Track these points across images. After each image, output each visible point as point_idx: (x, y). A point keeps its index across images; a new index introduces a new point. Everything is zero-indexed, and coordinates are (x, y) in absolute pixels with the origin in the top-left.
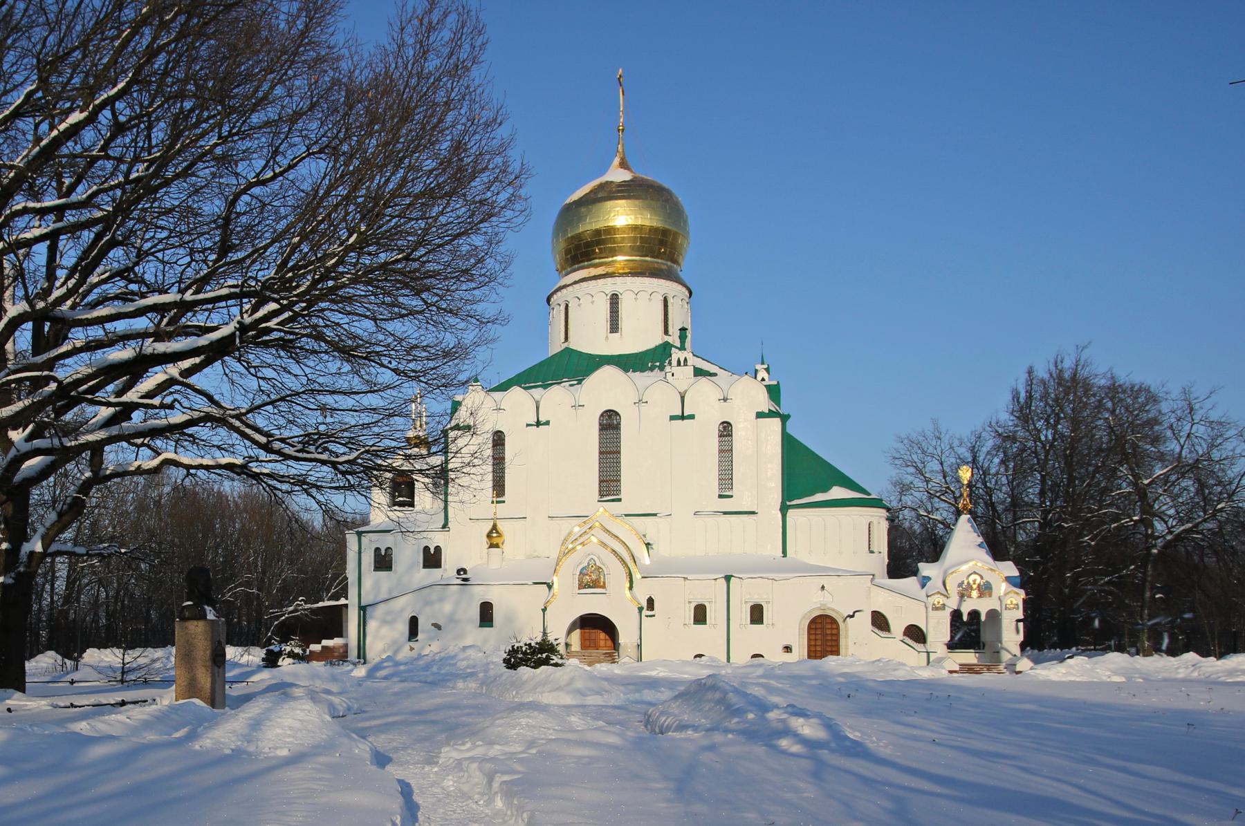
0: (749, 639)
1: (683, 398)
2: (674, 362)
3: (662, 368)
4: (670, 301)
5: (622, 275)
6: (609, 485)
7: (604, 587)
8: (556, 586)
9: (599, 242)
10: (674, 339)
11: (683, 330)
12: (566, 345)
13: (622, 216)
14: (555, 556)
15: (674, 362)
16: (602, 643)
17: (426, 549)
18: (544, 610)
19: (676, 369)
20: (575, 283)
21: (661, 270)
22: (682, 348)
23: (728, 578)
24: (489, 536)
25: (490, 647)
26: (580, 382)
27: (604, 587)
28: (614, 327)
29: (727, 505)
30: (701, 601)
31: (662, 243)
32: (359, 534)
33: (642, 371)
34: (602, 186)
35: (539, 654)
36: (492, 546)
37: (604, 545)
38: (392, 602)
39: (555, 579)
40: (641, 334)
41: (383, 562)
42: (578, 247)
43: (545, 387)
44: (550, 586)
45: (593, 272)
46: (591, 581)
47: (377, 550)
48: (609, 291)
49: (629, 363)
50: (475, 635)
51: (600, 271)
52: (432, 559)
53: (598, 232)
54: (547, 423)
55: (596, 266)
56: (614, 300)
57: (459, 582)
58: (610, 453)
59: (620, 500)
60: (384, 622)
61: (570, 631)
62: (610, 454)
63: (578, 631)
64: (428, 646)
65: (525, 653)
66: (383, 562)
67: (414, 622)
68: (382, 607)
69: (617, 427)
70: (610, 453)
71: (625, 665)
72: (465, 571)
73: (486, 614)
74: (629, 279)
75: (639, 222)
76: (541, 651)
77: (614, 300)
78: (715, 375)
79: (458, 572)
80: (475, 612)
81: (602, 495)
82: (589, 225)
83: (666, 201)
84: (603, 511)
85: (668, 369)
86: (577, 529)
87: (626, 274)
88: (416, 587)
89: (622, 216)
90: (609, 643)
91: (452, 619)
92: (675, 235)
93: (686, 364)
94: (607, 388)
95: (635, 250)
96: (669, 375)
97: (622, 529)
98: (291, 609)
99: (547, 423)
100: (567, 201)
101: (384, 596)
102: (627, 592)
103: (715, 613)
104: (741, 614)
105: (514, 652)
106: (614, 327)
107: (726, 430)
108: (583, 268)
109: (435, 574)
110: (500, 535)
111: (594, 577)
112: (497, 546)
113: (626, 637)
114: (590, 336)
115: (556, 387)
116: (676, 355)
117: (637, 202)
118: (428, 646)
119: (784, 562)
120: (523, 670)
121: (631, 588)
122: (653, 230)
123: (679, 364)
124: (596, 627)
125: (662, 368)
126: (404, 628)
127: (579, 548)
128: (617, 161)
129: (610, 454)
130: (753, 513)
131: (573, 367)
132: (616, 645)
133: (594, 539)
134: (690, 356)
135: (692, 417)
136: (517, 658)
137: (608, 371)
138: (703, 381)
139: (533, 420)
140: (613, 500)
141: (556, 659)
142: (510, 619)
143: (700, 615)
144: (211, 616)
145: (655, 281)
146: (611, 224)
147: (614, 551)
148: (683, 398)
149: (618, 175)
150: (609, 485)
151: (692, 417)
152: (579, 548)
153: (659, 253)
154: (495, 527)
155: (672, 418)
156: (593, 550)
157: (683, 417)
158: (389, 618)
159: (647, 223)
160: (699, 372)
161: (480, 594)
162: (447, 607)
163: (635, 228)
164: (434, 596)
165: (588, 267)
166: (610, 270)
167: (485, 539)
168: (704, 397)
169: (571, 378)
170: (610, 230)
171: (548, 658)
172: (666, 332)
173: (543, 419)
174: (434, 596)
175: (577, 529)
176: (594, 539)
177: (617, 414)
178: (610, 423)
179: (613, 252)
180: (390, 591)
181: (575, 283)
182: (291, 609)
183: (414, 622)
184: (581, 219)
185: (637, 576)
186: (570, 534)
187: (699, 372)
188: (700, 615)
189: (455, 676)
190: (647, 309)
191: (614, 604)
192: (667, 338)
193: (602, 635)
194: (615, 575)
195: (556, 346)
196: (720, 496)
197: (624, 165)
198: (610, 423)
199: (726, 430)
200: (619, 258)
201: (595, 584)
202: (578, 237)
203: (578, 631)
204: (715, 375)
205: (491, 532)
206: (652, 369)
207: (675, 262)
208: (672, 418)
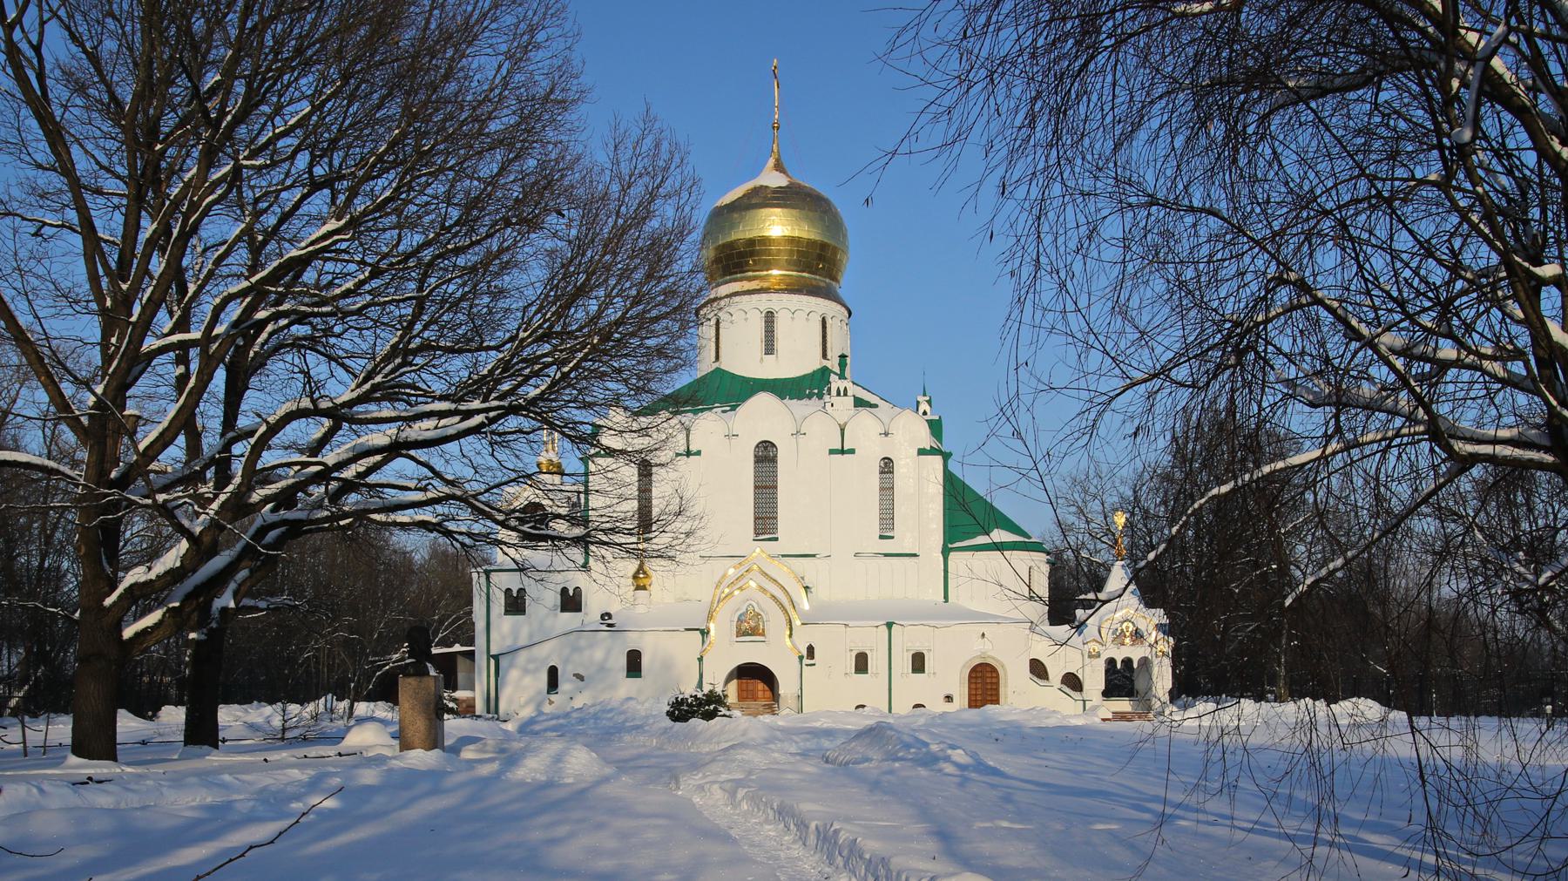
0: (911, 690)
1: (842, 431)
2: (834, 392)
3: (820, 396)
4: (829, 322)
5: (777, 291)
6: (765, 523)
8: (712, 633)
9: (752, 254)
10: (833, 364)
11: (843, 357)
13: (777, 225)
14: (707, 599)
15: (834, 392)
16: (760, 694)
17: (564, 591)
18: (700, 659)
19: (835, 400)
22: (842, 376)
23: (889, 625)
24: (635, 577)
25: (646, 699)
26: (733, 408)
28: (770, 348)
29: (888, 546)
30: (862, 649)
31: (821, 258)
32: (487, 573)
33: (800, 398)
34: (757, 191)
35: (707, 706)
36: (638, 588)
37: (763, 590)
38: (535, 649)
39: (712, 626)
40: (797, 355)
41: (515, 604)
42: (729, 257)
43: (695, 412)
44: (704, 633)
45: (747, 285)
46: (749, 628)
47: (508, 591)
48: (764, 307)
50: (627, 687)
52: (571, 601)
53: (751, 242)
54: (698, 453)
55: (750, 279)
56: (770, 318)
60: (526, 671)
61: (728, 681)
62: (766, 489)
65: (690, 705)
66: (515, 604)
67: (553, 673)
68: (522, 657)
69: (774, 460)
71: (785, 716)
72: (609, 615)
73: (634, 664)
74: (785, 297)
75: (796, 234)
77: (770, 318)
78: (876, 406)
79: (602, 617)
80: (623, 661)
81: (757, 534)
83: (825, 212)
84: (759, 551)
85: (827, 398)
86: (731, 571)
88: (560, 631)
89: (777, 225)
90: (769, 694)
91: (602, 669)
92: (835, 250)
94: (763, 417)
95: (791, 264)
97: (780, 570)
98: (395, 657)
99: (698, 453)
100: (718, 204)
101: (522, 642)
103: (876, 662)
104: (903, 662)
106: (770, 348)
107: (887, 466)
108: (736, 280)
110: (647, 575)
111: (752, 624)
112: (644, 588)
113: (786, 687)
115: (706, 414)
117: (794, 212)
119: (946, 611)
120: (696, 722)
122: (811, 243)
123: (838, 394)
124: (754, 676)
125: (820, 396)
126: (544, 677)
128: (771, 162)
129: (766, 489)
130: (915, 555)
131: (729, 391)
134: (849, 385)
135: (852, 451)
136: (681, 711)
137: (764, 400)
138: (864, 413)
139: (682, 449)
141: (723, 711)
142: (667, 666)
143: (861, 663)
144: (433, 673)
145: (812, 300)
148: (842, 431)
149: (773, 179)
150: (765, 523)
151: (852, 451)
153: (817, 268)
155: (832, 452)
157: (842, 452)
158: (531, 666)
159: (805, 235)
161: (633, 641)
162: (599, 654)
163: (792, 240)
164: (583, 643)
165: (741, 280)
166: (765, 285)
169: (723, 403)
170: (765, 241)
171: (716, 710)
172: (824, 356)
173: (693, 448)
174: (583, 643)
175: (731, 571)
176: (753, 584)
177: (773, 445)
178: (766, 455)
179: (768, 265)
180: (531, 636)
182: (395, 657)
184: (733, 226)
185: (797, 622)
186: (724, 576)
187: (859, 403)
188: (861, 663)
189: (620, 729)
190: (801, 331)
191: (775, 653)
192: (825, 363)
193: (761, 686)
194: (774, 621)
195: (705, 366)
196: (881, 537)
197: (779, 167)
198: (766, 455)
199: (887, 466)
200: (775, 272)
201: (754, 631)
204: (876, 406)
205: (638, 572)
206: (810, 397)
207: (835, 279)
208: (832, 452)
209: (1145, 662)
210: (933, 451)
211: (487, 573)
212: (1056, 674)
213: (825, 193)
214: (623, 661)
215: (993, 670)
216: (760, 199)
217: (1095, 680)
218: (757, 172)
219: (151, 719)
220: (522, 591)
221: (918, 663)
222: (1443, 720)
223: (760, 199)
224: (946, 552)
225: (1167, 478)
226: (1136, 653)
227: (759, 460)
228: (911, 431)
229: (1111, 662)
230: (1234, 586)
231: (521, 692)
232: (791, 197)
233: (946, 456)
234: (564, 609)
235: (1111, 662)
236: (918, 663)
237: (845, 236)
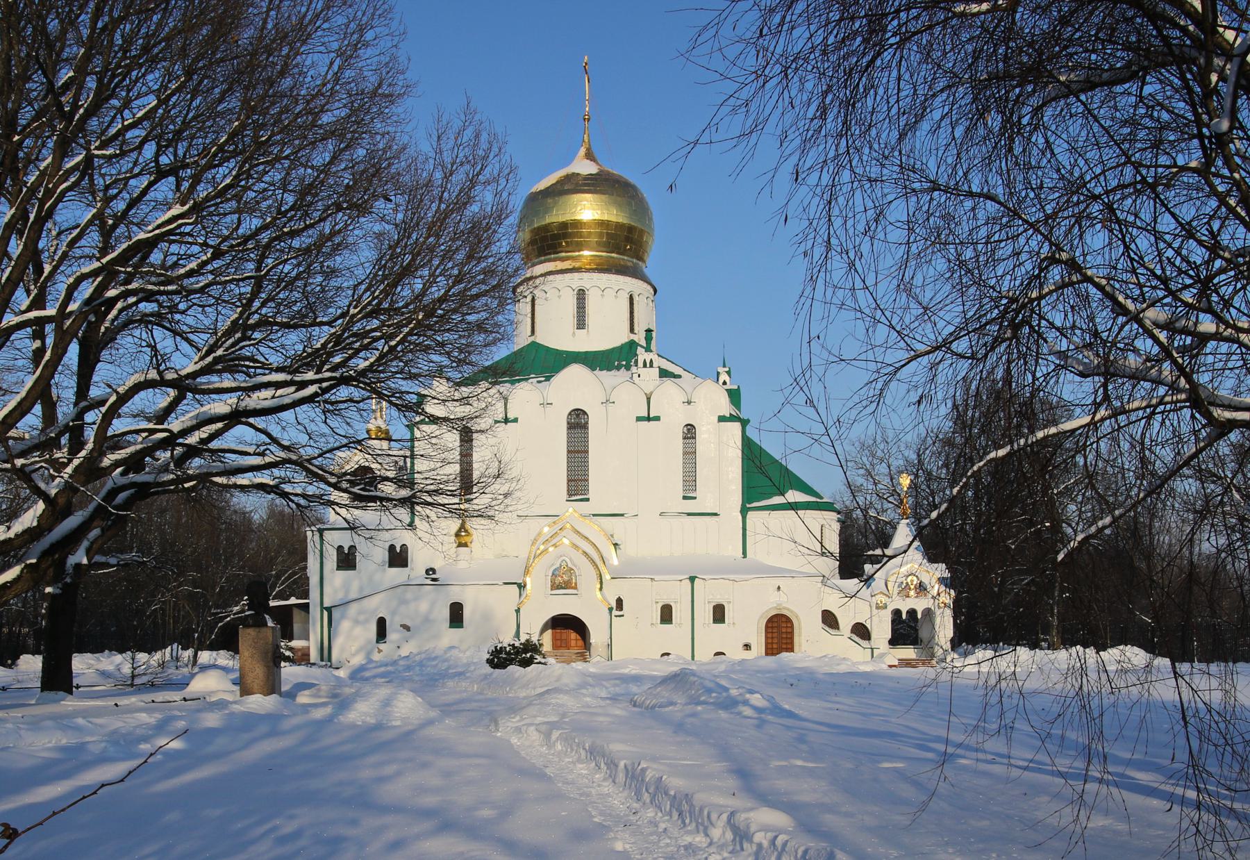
0: (712, 638)
1: (649, 399)
2: (640, 364)
3: (628, 368)
4: (636, 299)
5: (588, 270)
6: (577, 485)
7: (575, 588)
8: (528, 587)
9: (565, 236)
10: (640, 338)
11: (649, 331)
12: (532, 339)
13: (587, 210)
14: (524, 555)
15: (640, 364)
16: (573, 643)
17: (392, 548)
18: (518, 611)
19: (642, 371)
21: (627, 267)
22: (648, 349)
23: (692, 579)
24: (457, 535)
25: (468, 648)
26: (548, 379)
27: (575, 588)
28: (581, 324)
29: (691, 506)
30: (667, 602)
31: (628, 240)
32: (321, 531)
33: (609, 370)
34: (569, 178)
35: (524, 654)
36: (460, 545)
37: (575, 546)
38: (365, 601)
39: (528, 580)
40: (606, 332)
41: (347, 560)
42: (544, 239)
43: (513, 383)
44: (522, 587)
46: (563, 582)
47: (340, 548)
49: (597, 361)
50: (451, 636)
51: (567, 265)
52: (398, 558)
53: (564, 225)
54: (516, 420)
55: (563, 259)
56: (581, 295)
57: (429, 582)
58: (578, 452)
59: (588, 500)
60: (357, 622)
61: (543, 631)
62: (578, 453)
63: (550, 631)
64: (399, 646)
65: (508, 653)
66: (347, 560)
67: (381, 623)
68: (353, 609)
69: (585, 426)
70: (578, 452)
71: (596, 663)
72: (434, 571)
73: (456, 615)
74: (596, 275)
75: (606, 218)
76: (525, 650)
77: (581, 295)
78: (679, 377)
79: (427, 572)
80: (446, 613)
81: (570, 495)
82: (556, 217)
83: (632, 197)
84: (572, 510)
85: (634, 369)
87: (593, 270)
88: (387, 585)
89: (587, 210)
90: (581, 643)
91: (427, 620)
92: (642, 232)
93: (651, 366)
94: (574, 387)
95: (600, 246)
96: (635, 376)
97: (592, 529)
98: (236, 609)
99: (516, 420)
100: (534, 190)
101: (353, 596)
102: (598, 593)
105: (497, 652)
106: (581, 324)
107: (690, 432)
108: (550, 260)
109: (396, 574)
110: (468, 534)
111: (566, 578)
112: (465, 545)
113: (597, 637)
114: (557, 331)
115: (523, 384)
116: (642, 355)
117: (603, 197)
118: (399, 646)
119: (745, 565)
120: (514, 669)
121: (601, 589)
122: (619, 226)
123: (645, 366)
124: (568, 627)
125: (628, 368)
126: (373, 628)
127: (551, 549)
128: (582, 151)
129: (578, 453)
130: (716, 514)
131: (543, 363)
132: (586, 644)
133: (566, 541)
135: (657, 419)
136: (500, 659)
138: (668, 382)
139: (501, 416)
140: (581, 500)
141: (539, 658)
142: (487, 617)
143: (666, 615)
144: (270, 624)
145: (621, 278)
146: (578, 218)
147: (585, 553)
148: (649, 399)
149: (585, 168)
150: (577, 485)
151: (657, 419)
152: (551, 549)
153: (625, 249)
155: (639, 419)
156: (565, 550)
157: (649, 419)
159: (613, 219)
160: (664, 374)
161: (455, 595)
162: (424, 606)
163: (602, 223)
164: (409, 596)
165: (554, 260)
166: (577, 265)
167: (453, 538)
168: (669, 399)
169: (538, 374)
170: (577, 224)
171: (532, 657)
173: (511, 416)
174: (409, 596)
175: (546, 529)
176: (566, 541)
177: (585, 413)
178: (578, 422)
179: (580, 246)
180: (361, 589)
182: (236, 609)
183: (381, 623)
184: (548, 210)
185: (607, 577)
186: (539, 534)
187: (664, 374)
188: (666, 615)
189: (444, 676)
191: (586, 605)
192: (633, 337)
193: (573, 635)
194: (585, 576)
195: (522, 339)
196: (685, 498)
197: (590, 156)
198: (578, 422)
199: (690, 432)
200: (586, 253)
201: (567, 585)
202: (546, 228)
203: (550, 631)
204: (679, 377)
205: (460, 530)
206: (618, 368)
207: (641, 259)
208: (639, 419)
209: (928, 613)
210: (732, 418)
211: (321, 531)
212: (846, 623)
213: (632, 180)
215: (788, 620)
216: (572, 185)
217: (882, 630)
218: (569, 162)
219: (10, 667)
220: (352, 548)
221: (719, 614)
222: (1203, 666)
223: (572, 185)
224: (744, 511)
225: (949, 442)
226: (920, 605)
227: (571, 426)
228: (711, 400)
229: (897, 613)
230: (1012, 541)
231: (352, 641)
232: (602, 183)
233: (744, 423)
234: (391, 565)
235: (897, 613)
236: (719, 614)
237: (650, 219)
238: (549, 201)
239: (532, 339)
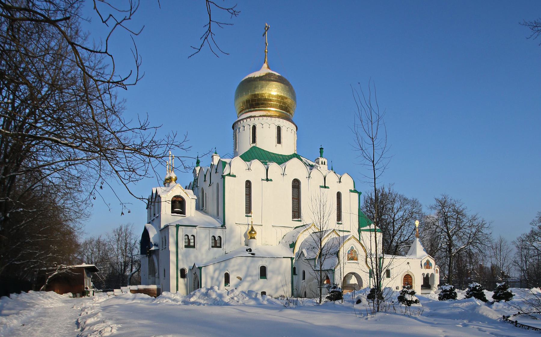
2: (320, 163)
7: (357, 260)
13: (273, 91)
15: (320, 163)
19: (321, 165)
20: (260, 116)
27: (357, 260)
28: (279, 141)
42: (253, 100)
54: (271, 180)
56: (279, 129)
59: (301, 221)
87: (279, 117)
89: (273, 91)
93: (324, 164)
95: (281, 108)
99: (271, 180)
106: (279, 141)
110: (256, 233)
112: (254, 238)
153: (286, 111)
154: (252, 230)
155: (321, 187)
157: (325, 187)
166: (269, 114)
178: (296, 184)
181: (260, 116)
198: (296, 184)
202: (255, 95)
209: (432, 275)
210: (355, 191)
214: (259, 271)
215: (411, 277)
216: (267, 78)
223: (267, 78)
224: (359, 231)
226: (430, 271)
228: (348, 182)
232: (280, 80)
233: (360, 194)
235: (423, 274)
238: (264, 82)
239: (254, 145)
